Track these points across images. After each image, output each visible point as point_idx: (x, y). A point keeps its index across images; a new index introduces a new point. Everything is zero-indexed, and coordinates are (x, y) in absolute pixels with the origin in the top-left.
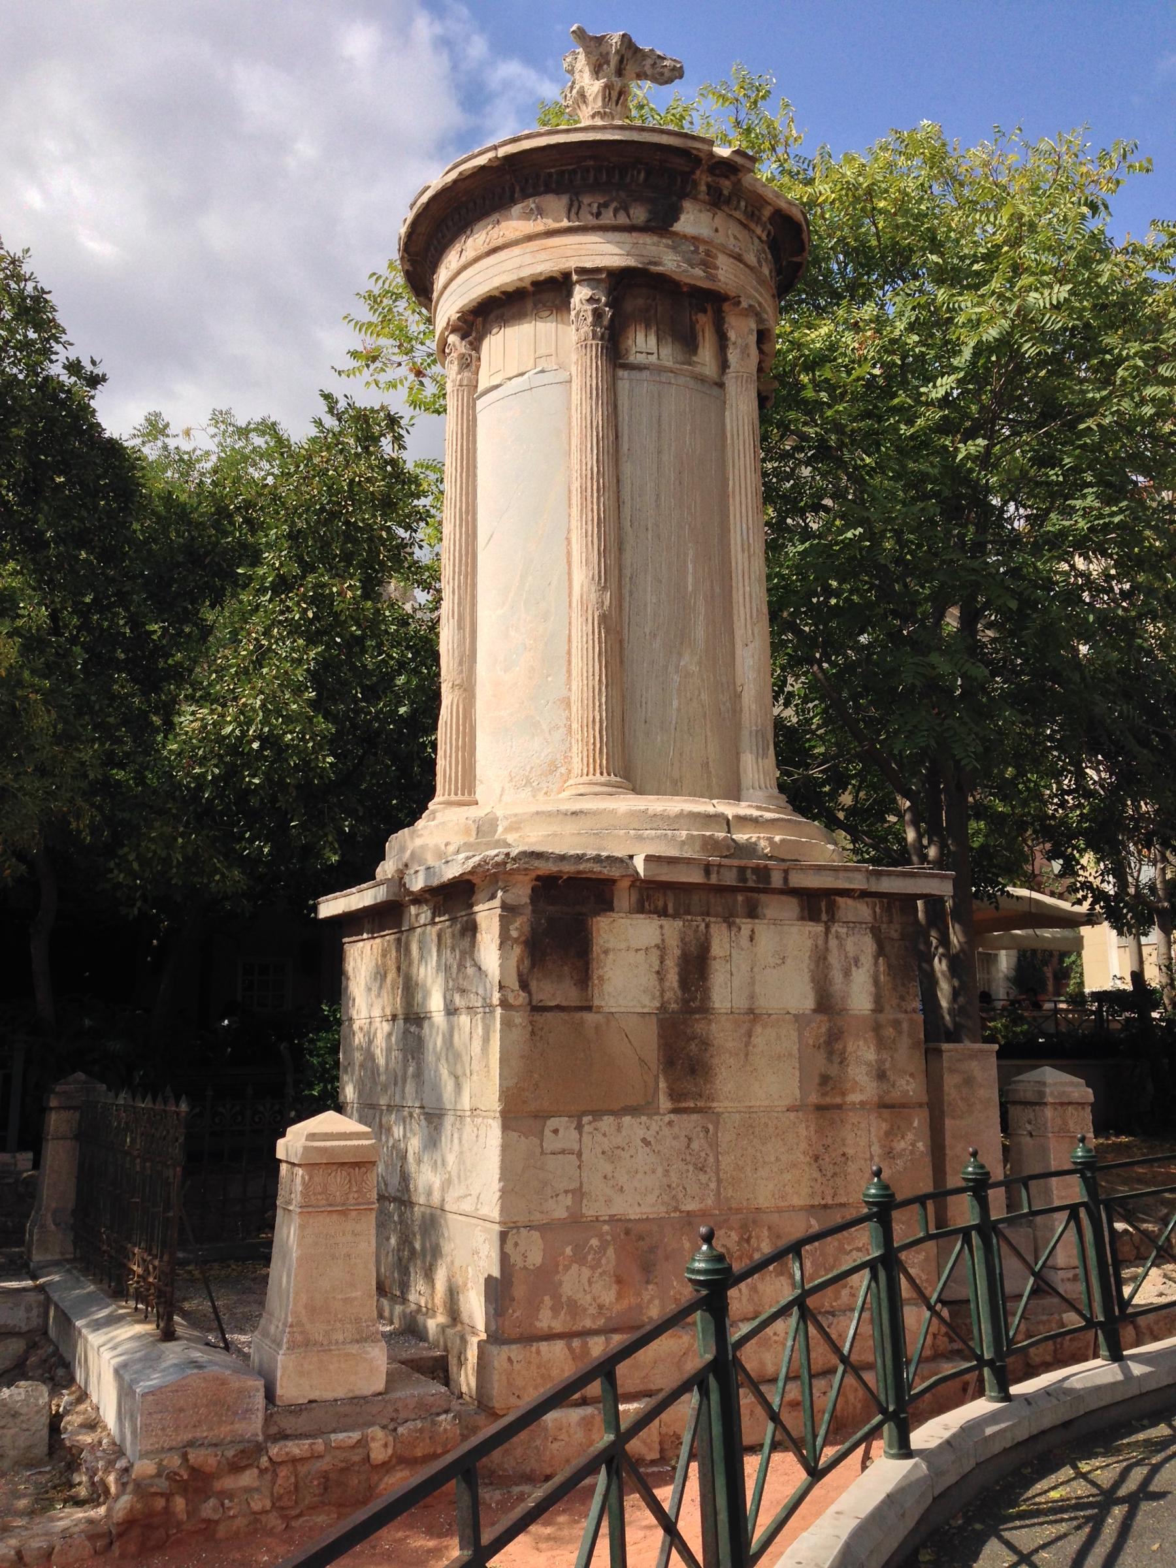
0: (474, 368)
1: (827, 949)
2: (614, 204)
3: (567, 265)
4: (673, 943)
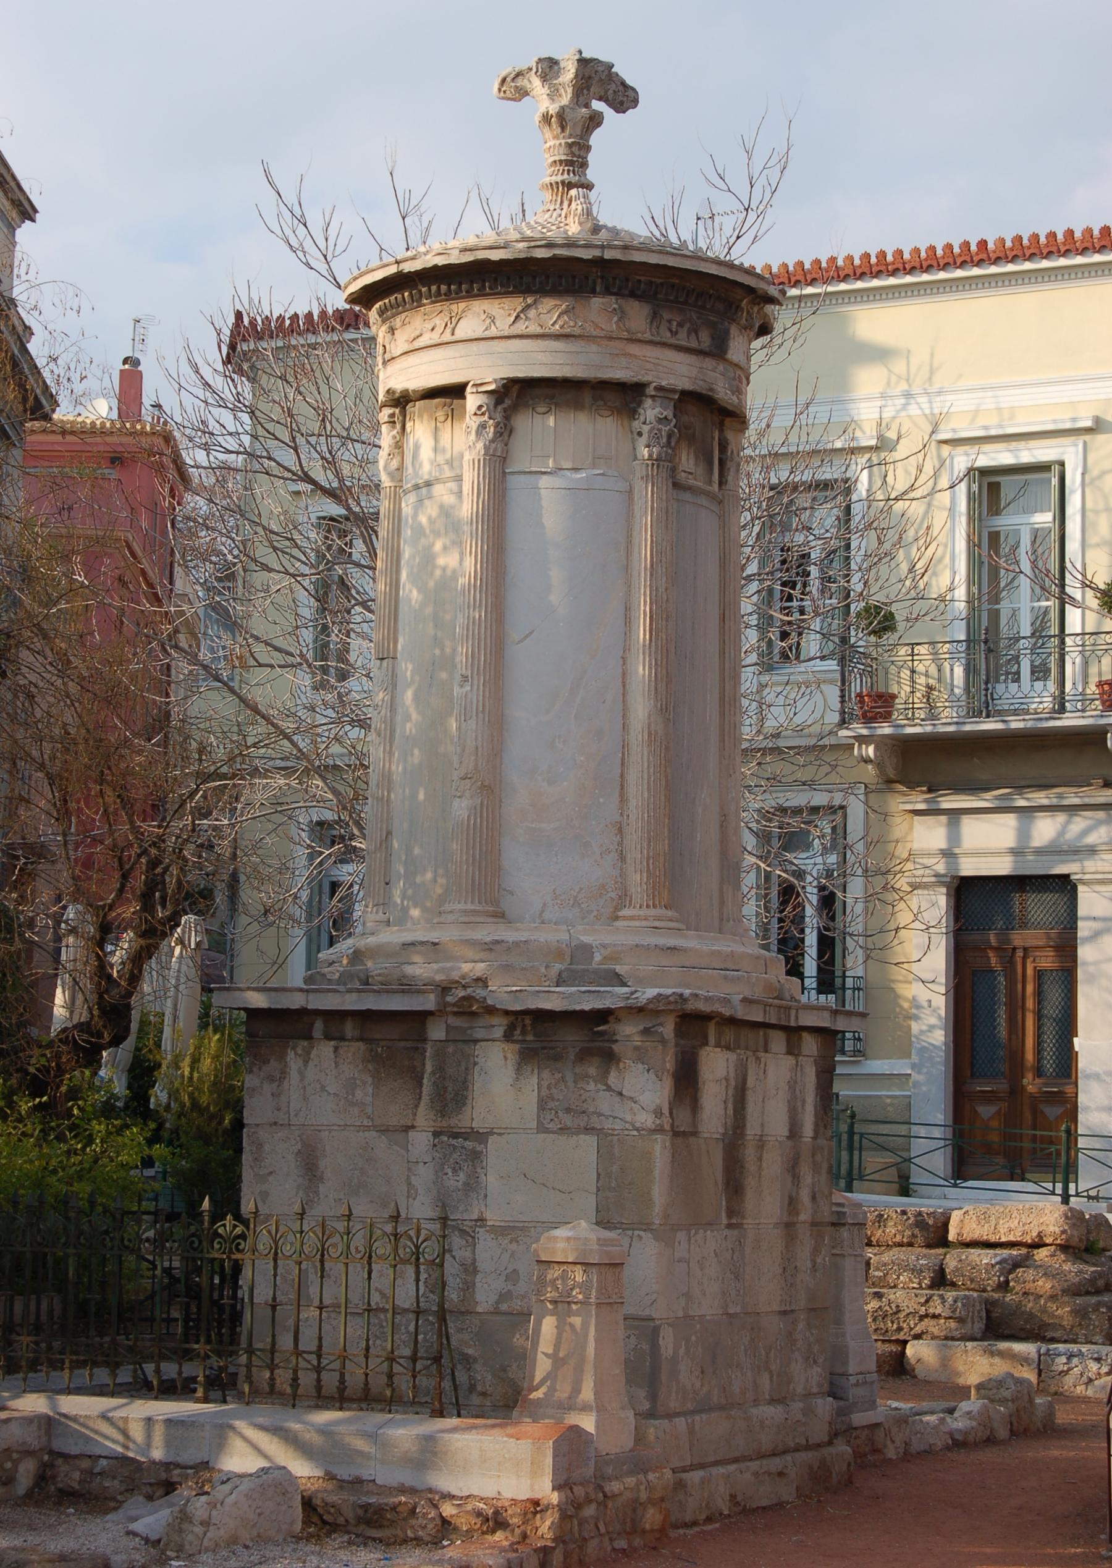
0: (506, 435)
1: (796, 1082)
2: (688, 325)
3: (645, 379)
4: (732, 1074)
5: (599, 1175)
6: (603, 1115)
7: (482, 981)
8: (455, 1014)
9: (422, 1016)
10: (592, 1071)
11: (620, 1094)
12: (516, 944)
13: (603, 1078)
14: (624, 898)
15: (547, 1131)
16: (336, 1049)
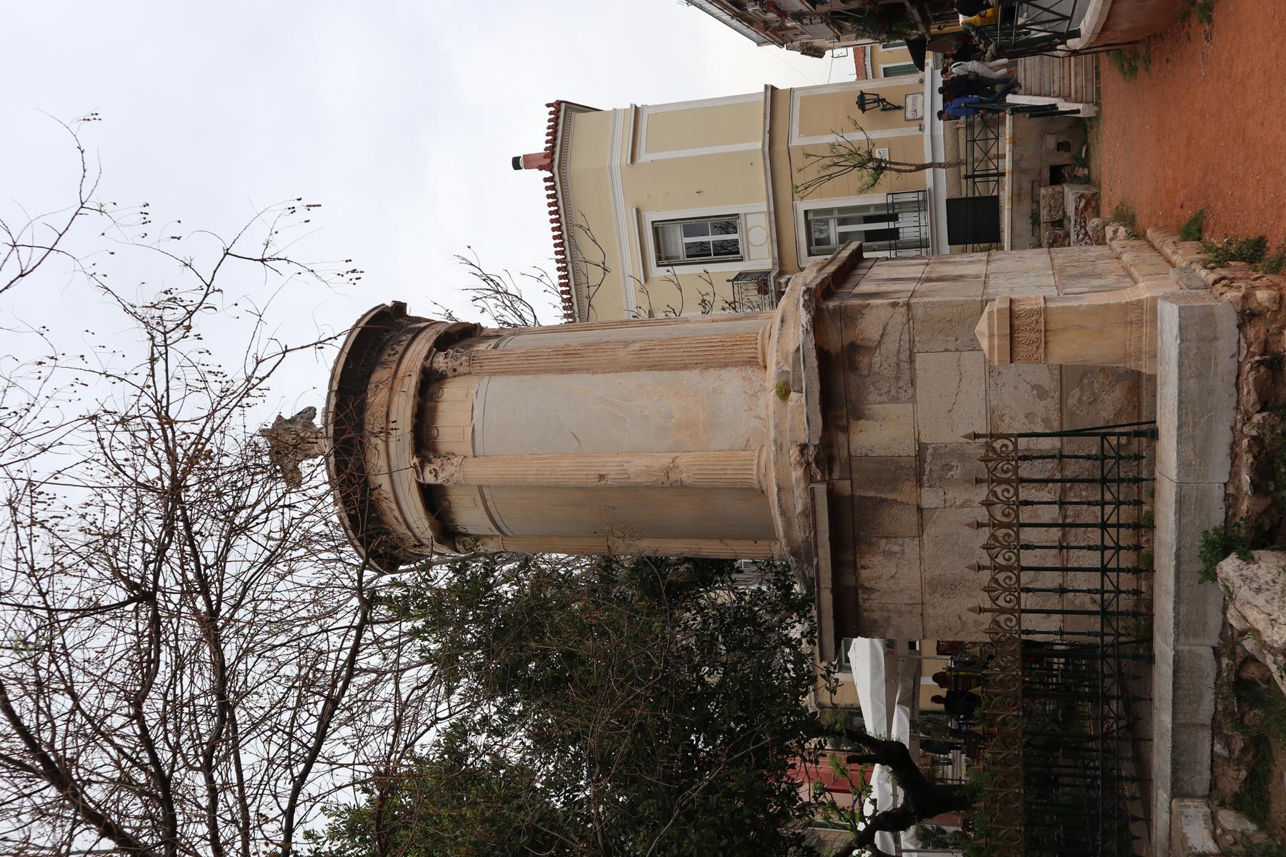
3: (419, 365)
5: (946, 350)
6: (899, 351)
7: (803, 448)
8: (830, 473)
9: (835, 500)
10: (866, 360)
11: (882, 336)
12: (776, 426)
13: (870, 350)
14: (751, 362)
15: (914, 395)
16: (863, 567)
